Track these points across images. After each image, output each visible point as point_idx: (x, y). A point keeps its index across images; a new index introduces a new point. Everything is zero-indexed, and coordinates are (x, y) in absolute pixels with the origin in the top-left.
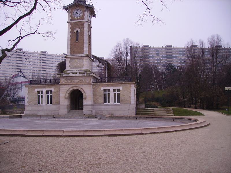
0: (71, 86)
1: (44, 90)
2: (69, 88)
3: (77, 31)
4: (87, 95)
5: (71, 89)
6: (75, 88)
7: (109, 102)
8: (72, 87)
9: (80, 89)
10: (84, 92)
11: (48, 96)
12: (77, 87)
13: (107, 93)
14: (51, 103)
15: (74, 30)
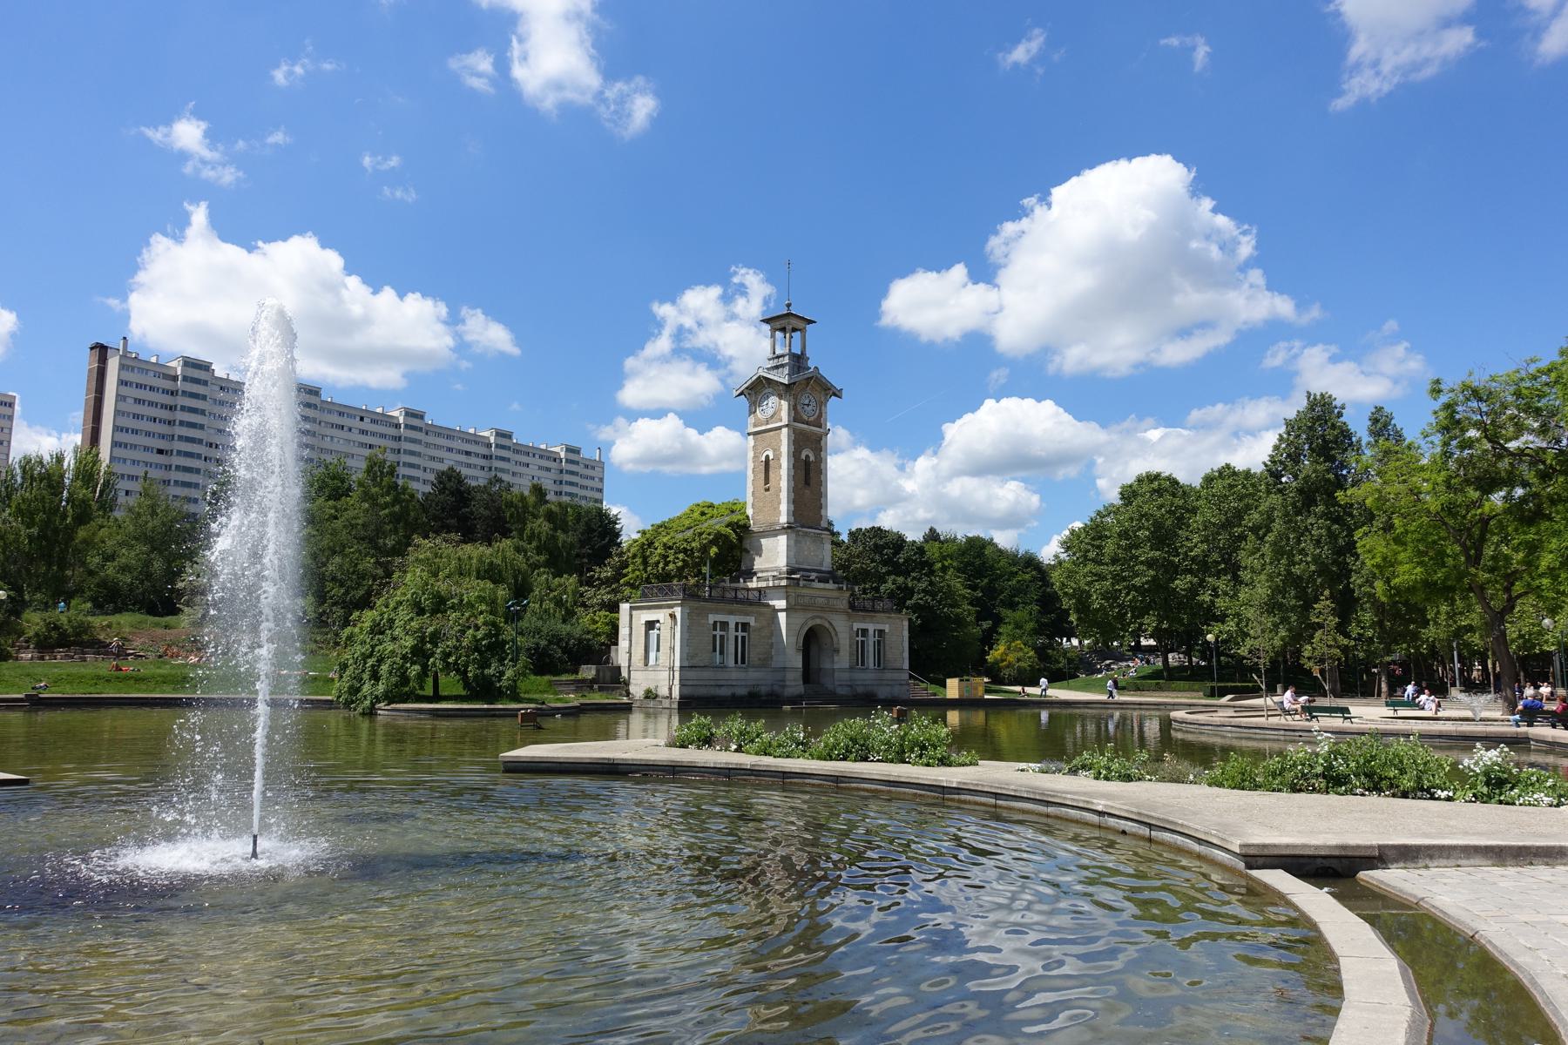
0: (810, 615)
1: (732, 620)
2: (802, 621)
3: (807, 456)
4: (842, 642)
5: (810, 624)
6: (818, 621)
7: (863, 664)
8: (813, 618)
9: (827, 625)
10: (836, 635)
11: (736, 637)
12: (821, 618)
13: (860, 639)
14: (743, 662)
15: (800, 453)
